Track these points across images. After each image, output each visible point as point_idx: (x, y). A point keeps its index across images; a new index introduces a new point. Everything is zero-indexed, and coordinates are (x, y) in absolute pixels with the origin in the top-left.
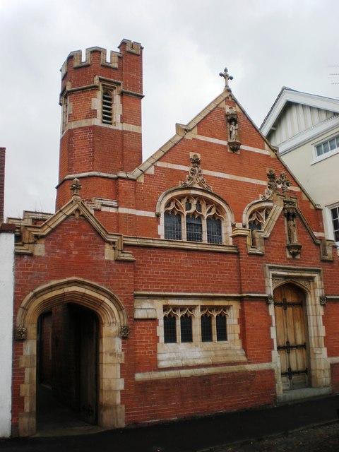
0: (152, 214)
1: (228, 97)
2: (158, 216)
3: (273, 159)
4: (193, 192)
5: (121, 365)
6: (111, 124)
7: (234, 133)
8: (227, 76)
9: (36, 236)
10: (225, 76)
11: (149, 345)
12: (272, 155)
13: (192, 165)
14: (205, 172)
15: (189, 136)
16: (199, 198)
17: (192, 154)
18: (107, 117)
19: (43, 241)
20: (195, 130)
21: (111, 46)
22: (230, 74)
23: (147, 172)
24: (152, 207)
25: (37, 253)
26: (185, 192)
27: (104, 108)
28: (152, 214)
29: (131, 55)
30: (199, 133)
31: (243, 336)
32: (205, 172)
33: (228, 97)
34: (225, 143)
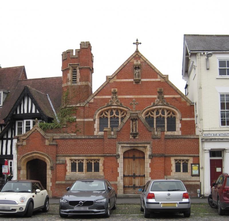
0: (92, 120)
1: (137, 55)
2: (94, 120)
3: (162, 82)
4: (112, 107)
5: (51, 178)
6: (76, 83)
7: (136, 74)
8: (138, 43)
9: (23, 139)
10: (137, 43)
11: (62, 172)
12: (162, 80)
13: (112, 94)
14: (120, 97)
15: (112, 81)
16: (117, 110)
17: (112, 90)
18: (74, 80)
19: (25, 140)
20: (115, 78)
21: (75, 47)
22: (139, 42)
23: (90, 102)
24: (92, 116)
25: (24, 144)
26: (108, 108)
27: (73, 76)
28: (92, 120)
29: (86, 49)
30: (118, 78)
31: (104, 170)
32: (120, 97)
33: (137, 55)
34: (132, 80)
